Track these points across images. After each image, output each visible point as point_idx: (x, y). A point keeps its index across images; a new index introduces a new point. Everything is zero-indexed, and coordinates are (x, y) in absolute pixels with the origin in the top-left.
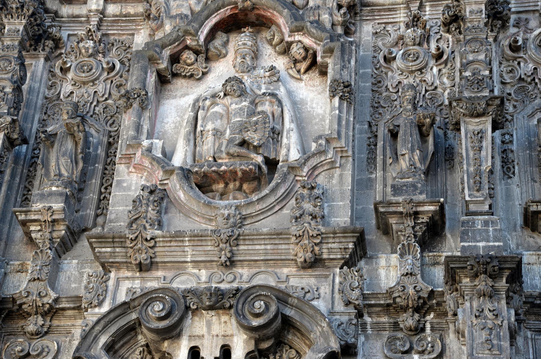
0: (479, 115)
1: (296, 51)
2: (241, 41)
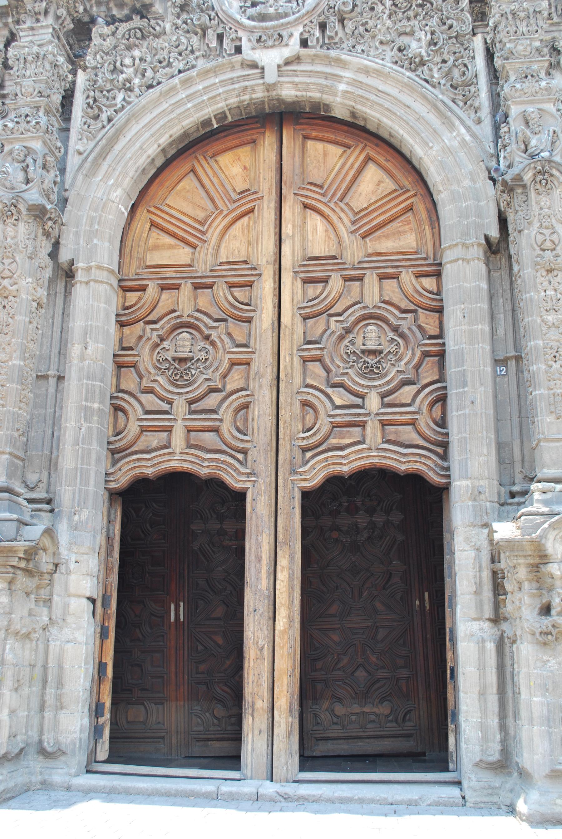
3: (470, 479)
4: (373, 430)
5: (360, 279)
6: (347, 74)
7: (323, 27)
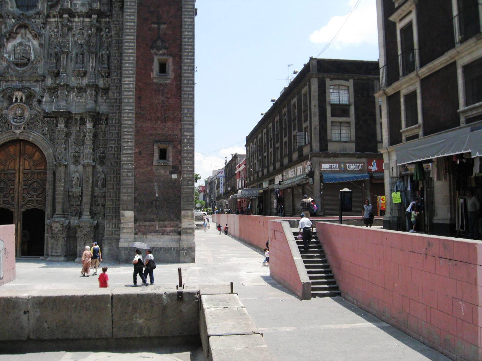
0: (64, 54)
1: (33, 34)
2: (23, 31)
3: (48, 211)
4: (35, 202)
5: (34, 174)
6: (32, 136)
7: (28, 125)
